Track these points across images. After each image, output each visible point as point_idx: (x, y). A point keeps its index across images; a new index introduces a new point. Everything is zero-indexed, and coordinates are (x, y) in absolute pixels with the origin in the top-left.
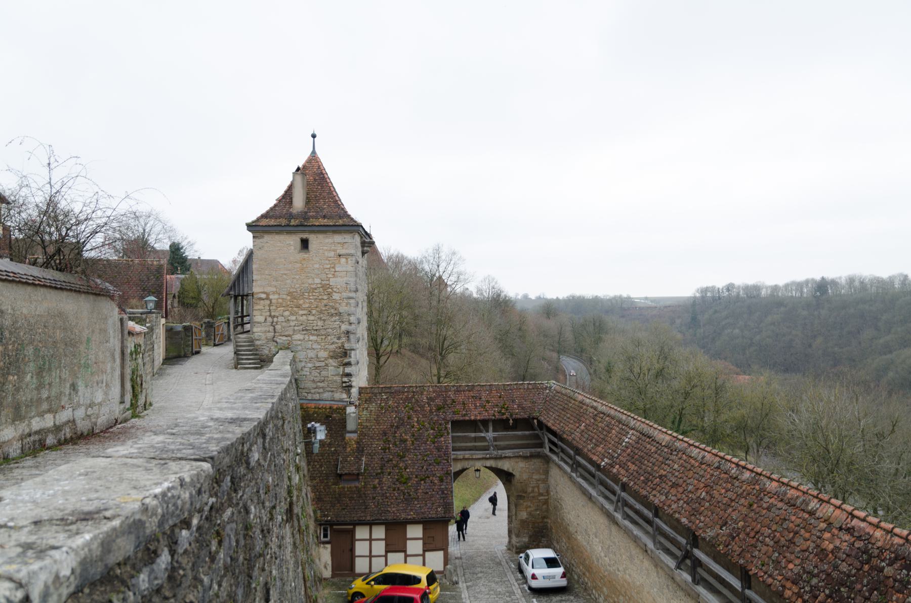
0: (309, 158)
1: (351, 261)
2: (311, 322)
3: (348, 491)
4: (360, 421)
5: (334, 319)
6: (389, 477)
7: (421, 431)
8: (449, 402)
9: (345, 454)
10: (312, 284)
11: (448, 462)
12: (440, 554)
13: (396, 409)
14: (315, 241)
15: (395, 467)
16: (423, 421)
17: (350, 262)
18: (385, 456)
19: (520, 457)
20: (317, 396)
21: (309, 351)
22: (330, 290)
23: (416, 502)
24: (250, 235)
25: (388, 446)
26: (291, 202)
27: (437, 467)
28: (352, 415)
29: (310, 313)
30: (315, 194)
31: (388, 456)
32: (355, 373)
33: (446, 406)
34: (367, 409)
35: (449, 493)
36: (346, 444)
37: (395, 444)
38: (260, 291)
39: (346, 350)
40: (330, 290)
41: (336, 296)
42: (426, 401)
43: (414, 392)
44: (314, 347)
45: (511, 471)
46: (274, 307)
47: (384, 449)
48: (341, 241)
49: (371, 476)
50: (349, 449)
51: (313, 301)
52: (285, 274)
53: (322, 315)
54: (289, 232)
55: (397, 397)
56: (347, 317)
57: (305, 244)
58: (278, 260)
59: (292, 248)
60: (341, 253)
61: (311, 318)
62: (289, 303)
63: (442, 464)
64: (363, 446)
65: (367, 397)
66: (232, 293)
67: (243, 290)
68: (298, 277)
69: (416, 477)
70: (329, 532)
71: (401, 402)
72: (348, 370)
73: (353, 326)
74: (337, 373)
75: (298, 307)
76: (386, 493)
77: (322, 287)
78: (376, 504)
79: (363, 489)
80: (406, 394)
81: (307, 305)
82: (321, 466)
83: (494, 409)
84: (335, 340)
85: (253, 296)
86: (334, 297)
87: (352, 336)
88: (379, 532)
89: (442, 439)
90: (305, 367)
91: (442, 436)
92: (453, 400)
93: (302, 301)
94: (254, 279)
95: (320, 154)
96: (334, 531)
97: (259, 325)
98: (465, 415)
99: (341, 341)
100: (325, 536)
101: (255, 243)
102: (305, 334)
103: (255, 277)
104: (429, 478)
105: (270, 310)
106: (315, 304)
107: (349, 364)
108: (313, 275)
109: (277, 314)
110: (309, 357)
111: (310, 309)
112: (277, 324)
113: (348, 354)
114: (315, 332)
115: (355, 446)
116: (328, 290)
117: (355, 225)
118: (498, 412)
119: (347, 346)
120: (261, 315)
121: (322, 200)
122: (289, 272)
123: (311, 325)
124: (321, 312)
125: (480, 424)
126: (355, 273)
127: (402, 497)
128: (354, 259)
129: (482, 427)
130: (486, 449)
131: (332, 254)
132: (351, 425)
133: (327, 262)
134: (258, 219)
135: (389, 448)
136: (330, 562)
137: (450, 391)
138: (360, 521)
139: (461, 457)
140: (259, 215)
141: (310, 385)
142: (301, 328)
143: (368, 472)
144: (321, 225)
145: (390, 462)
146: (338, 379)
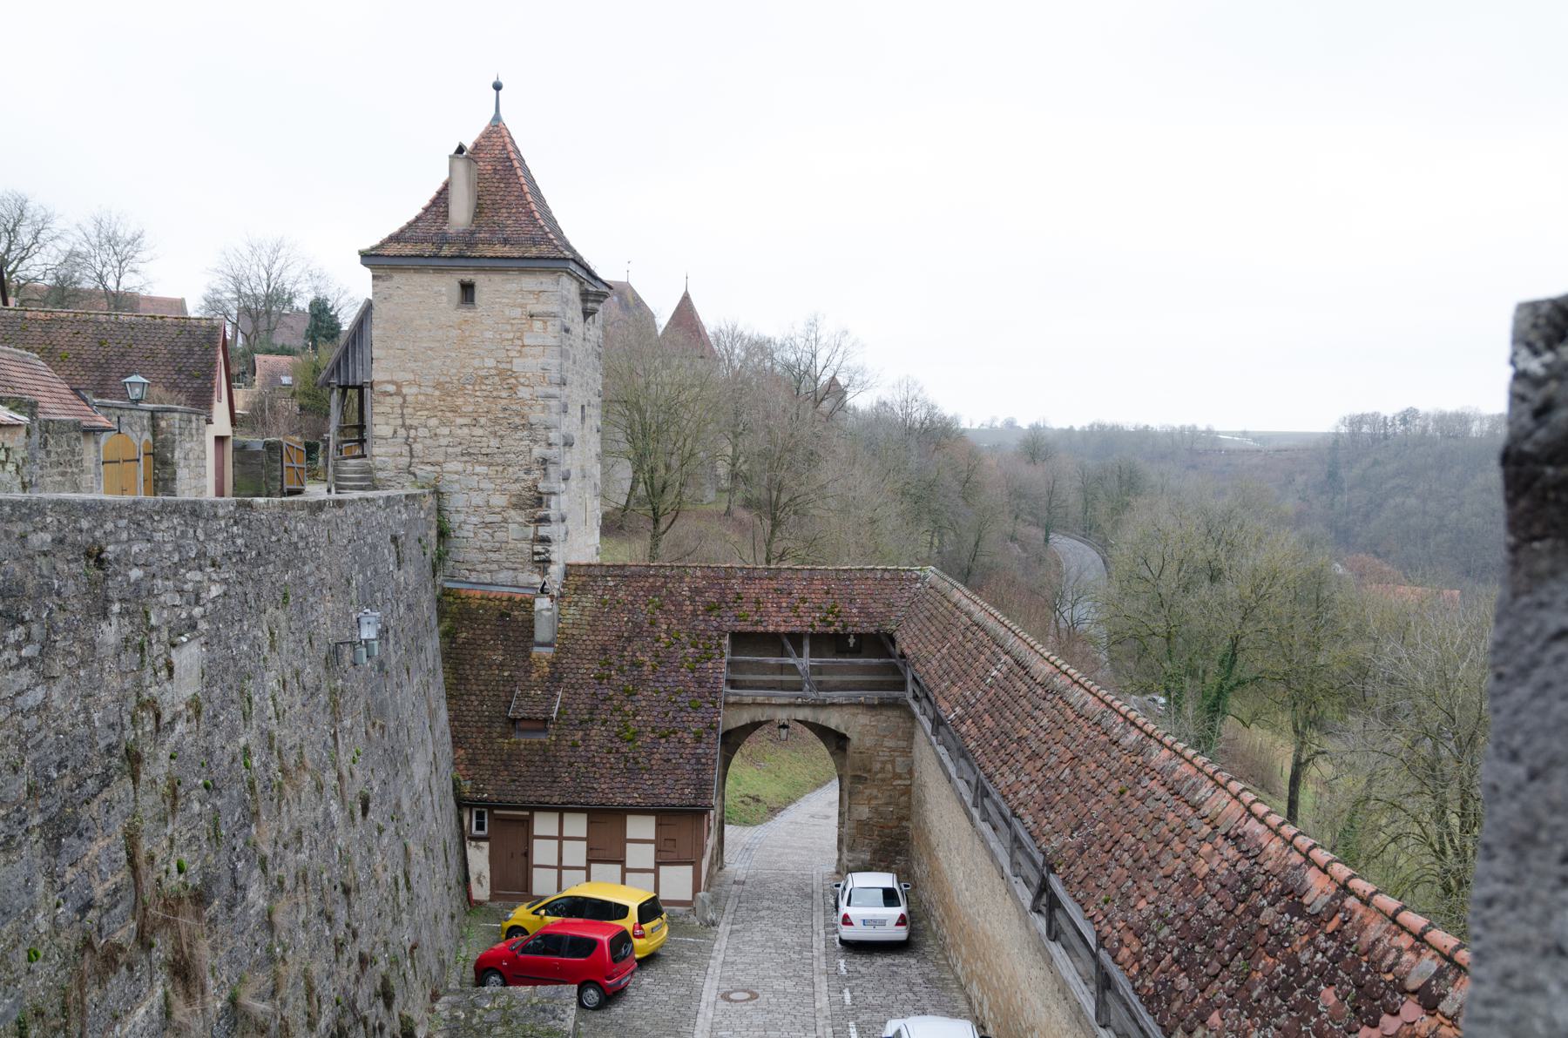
0: (487, 128)
1: (554, 327)
2: (478, 439)
3: (525, 749)
4: (561, 625)
5: (520, 434)
6: (603, 728)
7: (672, 649)
8: (730, 597)
9: (527, 683)
10: (479, 368)
11: (715, 707)
12: (689, 869)
13: (630, 607)
14: (486, 285)
15: (616, 711)
16: (678, 631)
17: (550, 329)
18: (600, 691)
19: (860, 704)
20: (487, 578)
21: (472, 494)
22: (513, 381)
23: (646, 776)
25: (607, 672)
26: (446, 214)
27: (693, 715)
28: (544, 613)
30: (493, 197)
31: (606, 691)
32: (556, 538)
33: (723, 605)
34: (576, 605)
35: (710, 762)
36: (531, 665)
37: (621, 670)
38: (385, 379)
39: (540, 493)
41: (524, 393)
42: (688, 594)
43: (666, 577)
44: (481, 486)
45: (842, 730)
47: (600, 678)
48: (535, 289)
49: (571, 724)
50: (535, 675)
51: (480, 400)
52: (431, 349)
53: (497, 428)
54: (439, 270)
55: (635, 584)
56: (543, 432)
57: (467, 290)
58: (418, 322)
59: (445, 299)
60: (533, 311)
61: (478, 432)
62: (437, 402)
63: (703, 710)
64: (562, 670)
65: (579, 583)
66: (334, 381)
67: (355, 377)
68: (454, 355)
69: (653, 731)
70: (486, 820)
71: (641, 593)
73: (555, 450)
74: (524, 536)
76: (594, 756)
77: (498, 375)
78: (574, 774)
79: (553, 748)
80: (651, 580)
81: (470, 409)
82: (482, 703)
83: (813, 614)
84: (521, 474)
85: (372, 388)
87: (551, 469)
88: (577, 825)
89: (710, 665)
90: (465, 522)
91: (709, 659)
92: (738, 593)
93: (462, 399)
95: (509, 120)
96: (496, 820)
97: (384, 441)
98: (757, 623)
99: (531, 477)
100: (480, 827)
101: (377, 289)
102: (466, 462)
103: (376, 353)
104: (676, 733)
105: (403, 415)
106: (485, 406)
107: (545, 520)
108: (481, 352)
109: (415, 423)
111: (475, 415)
112: (415, 442)
113: (545, 500)
114: (486, 459)
115: (548, 670)
116: (509, 381)
117: (560, 259)
118: (821, 621)
119: (542, 486)
120: (387, 424)
121: (504, 210)
124: (496, 421)
125: (786, 641)
127: (622, 766)
128: (558, 322)
129: (789, 647)
130: (798, 687)
131: (518, 312)
132: (543, 632)
133: (509, 327)
134: (383, 244)
135: (609, 677)
136: (487, 874)
137: (735, 578)
138: (540, 803)
139: (749, 700)
140: (386, 236)
141: (474, 556)
142: (459, 449)
143: (565, 717)
144: (497, 257)
145: (608, 702)
146: (525, 546)
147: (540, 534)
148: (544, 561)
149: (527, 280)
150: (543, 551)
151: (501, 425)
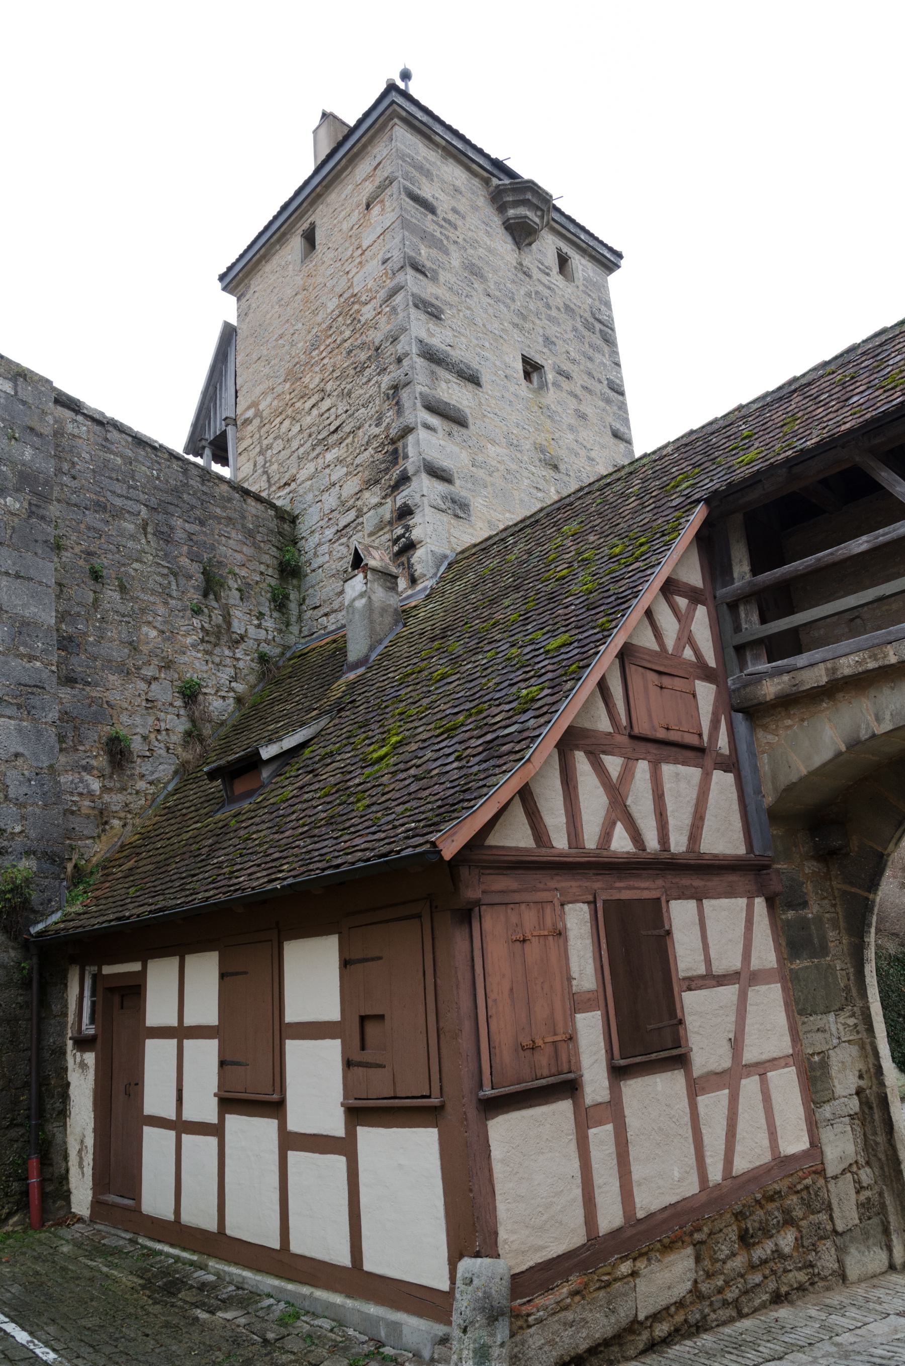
136: (90, 1141)
139: (818, 677)
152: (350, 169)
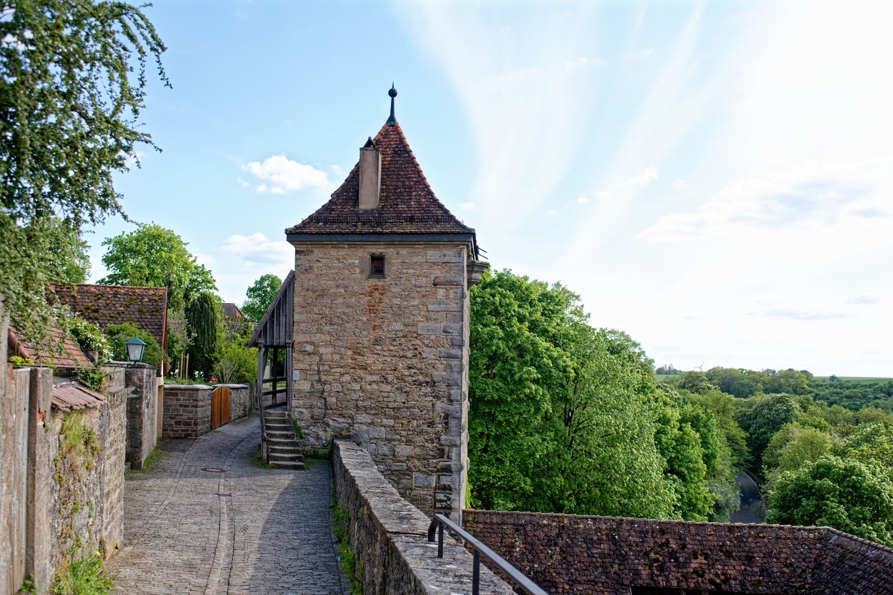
14: (395, 257)
17: (452, 296)
22: (418, 342)
24: (291, 249)
29: (385, 380)
38: (305, 340)
40: (418, 342)
46: (326, 368)
48: (439, 260)
53: (403, 384)
54: (353, 245)
61: (388, 388)
62: (350, 361)
66: (262, 341)
72: (445, 480)
75: (364, 368)
81: (380, 366)
86: (424, 355)
94: (295, 320)
101: (299, 262)
103: (297, 317)
107: (447, 470)
108: (389, 316)
109: (330, 378)
110: (380, 452)
117: (464, 233)
120: (306, 379)
122: (351, 310)
123: (385, 399)
126: (460, 314)
131: (423, 281)
134: (304, 224)
147: (442, 483)
148: (445, 508)
149: (432, 252)
150: (445, 499)
151: (406, 382)
152: (423, 246)
